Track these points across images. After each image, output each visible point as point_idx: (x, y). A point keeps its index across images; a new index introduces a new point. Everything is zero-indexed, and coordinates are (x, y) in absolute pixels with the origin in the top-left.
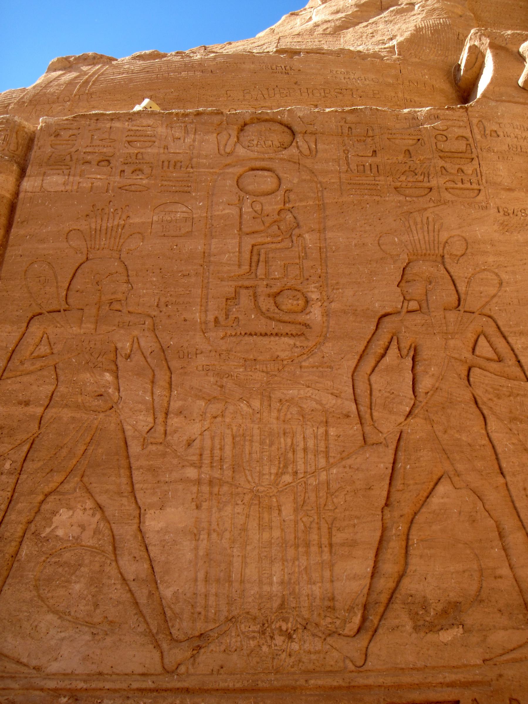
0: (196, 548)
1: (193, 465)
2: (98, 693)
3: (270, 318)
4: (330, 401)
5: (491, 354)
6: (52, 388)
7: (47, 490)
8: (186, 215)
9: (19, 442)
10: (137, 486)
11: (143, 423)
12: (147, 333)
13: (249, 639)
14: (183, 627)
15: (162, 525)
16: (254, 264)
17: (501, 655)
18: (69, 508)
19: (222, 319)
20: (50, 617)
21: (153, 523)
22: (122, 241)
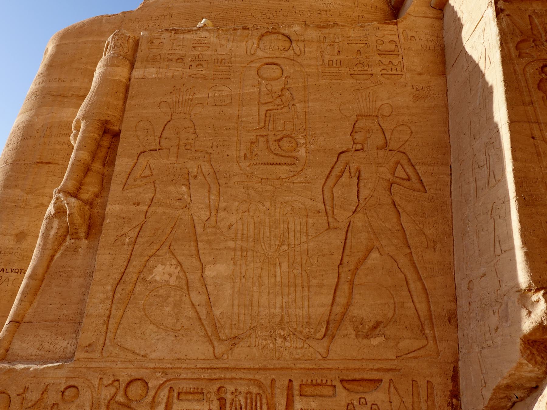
0: (233, 287)
1: (232, 239)
2: (178, 370)
3: (276, 154)
4: (309, 203)
5: (405, 176)
6: (152, 195)
7: (150, 254)
8: (228, 93)
9: (134, 226)
10: (200, 252)
11: (204, 216)
12: (206, 163)
13: (263, 339)
14: (226, 332)
15: (215, 273)
16: (267, 122)
17: (407, 354)
18: (163, 264)
19: (248, 155)
20: (151, 326)
21: (209, 273)
22: (191, 108)
